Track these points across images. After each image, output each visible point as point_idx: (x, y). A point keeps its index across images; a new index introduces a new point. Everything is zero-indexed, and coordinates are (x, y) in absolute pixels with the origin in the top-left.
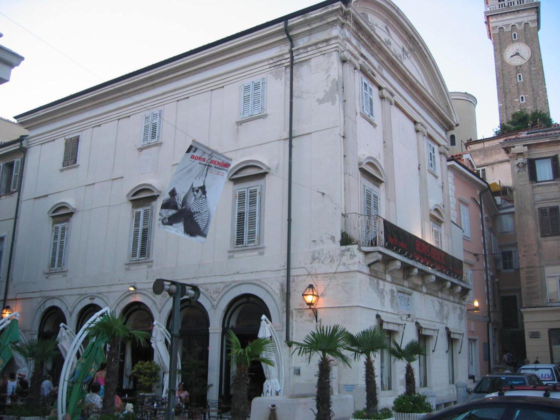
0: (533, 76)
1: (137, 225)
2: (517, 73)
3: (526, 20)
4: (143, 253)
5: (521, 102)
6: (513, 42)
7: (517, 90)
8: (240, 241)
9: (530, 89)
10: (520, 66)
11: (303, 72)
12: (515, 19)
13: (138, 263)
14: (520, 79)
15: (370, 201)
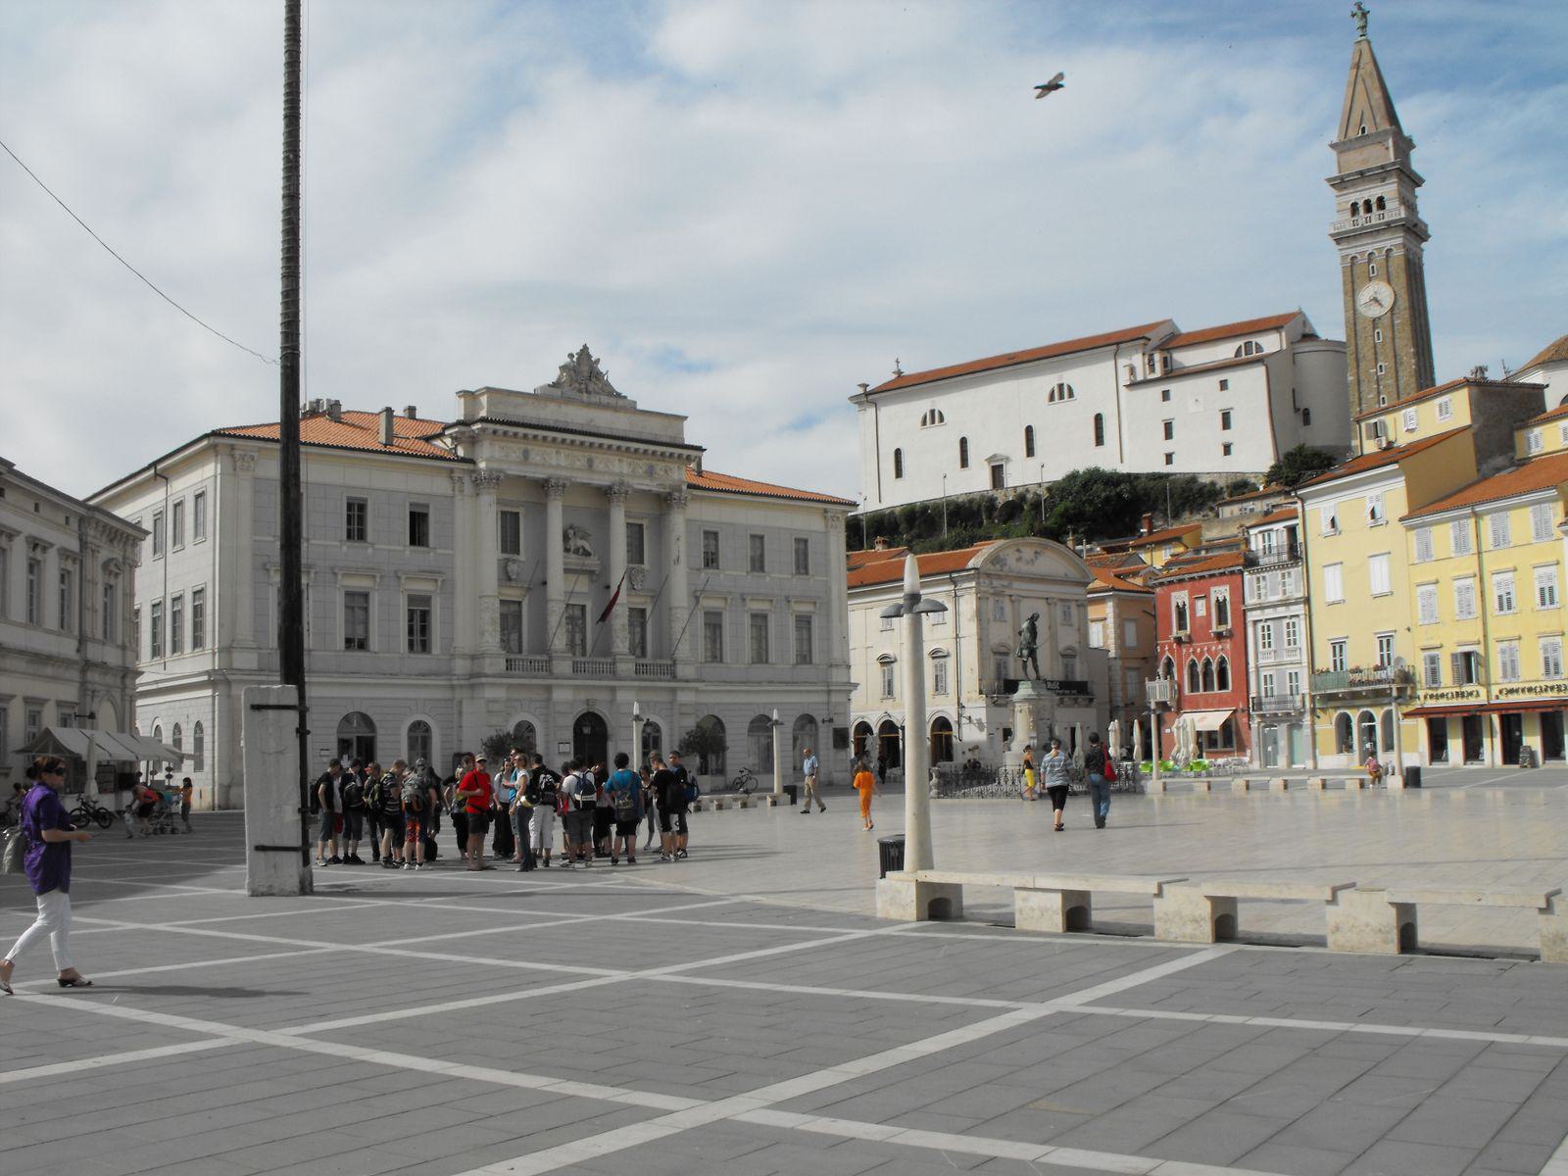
0: (1396, 333)
1: (884, 677)
2: (1374, 328)
3: (1388, 245)
4: (890, 692)
5: (1379, 374)
6: (1370, 279)
7: (1373, 356)
8: (937, 690)
9: (1391, 354)
10: (1379, 318)
11: (962, 600)
12: (1372, 243)
13: (887, 698)
14: (1379, 339)
15: (1000, 668)
